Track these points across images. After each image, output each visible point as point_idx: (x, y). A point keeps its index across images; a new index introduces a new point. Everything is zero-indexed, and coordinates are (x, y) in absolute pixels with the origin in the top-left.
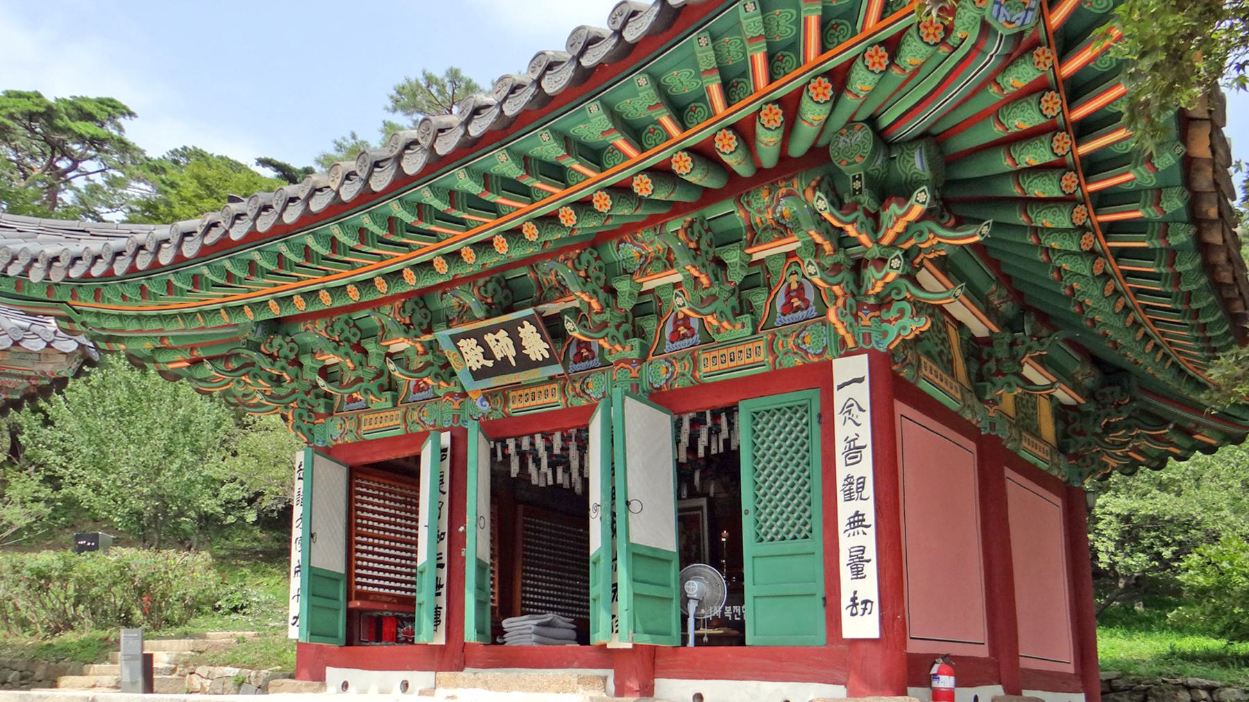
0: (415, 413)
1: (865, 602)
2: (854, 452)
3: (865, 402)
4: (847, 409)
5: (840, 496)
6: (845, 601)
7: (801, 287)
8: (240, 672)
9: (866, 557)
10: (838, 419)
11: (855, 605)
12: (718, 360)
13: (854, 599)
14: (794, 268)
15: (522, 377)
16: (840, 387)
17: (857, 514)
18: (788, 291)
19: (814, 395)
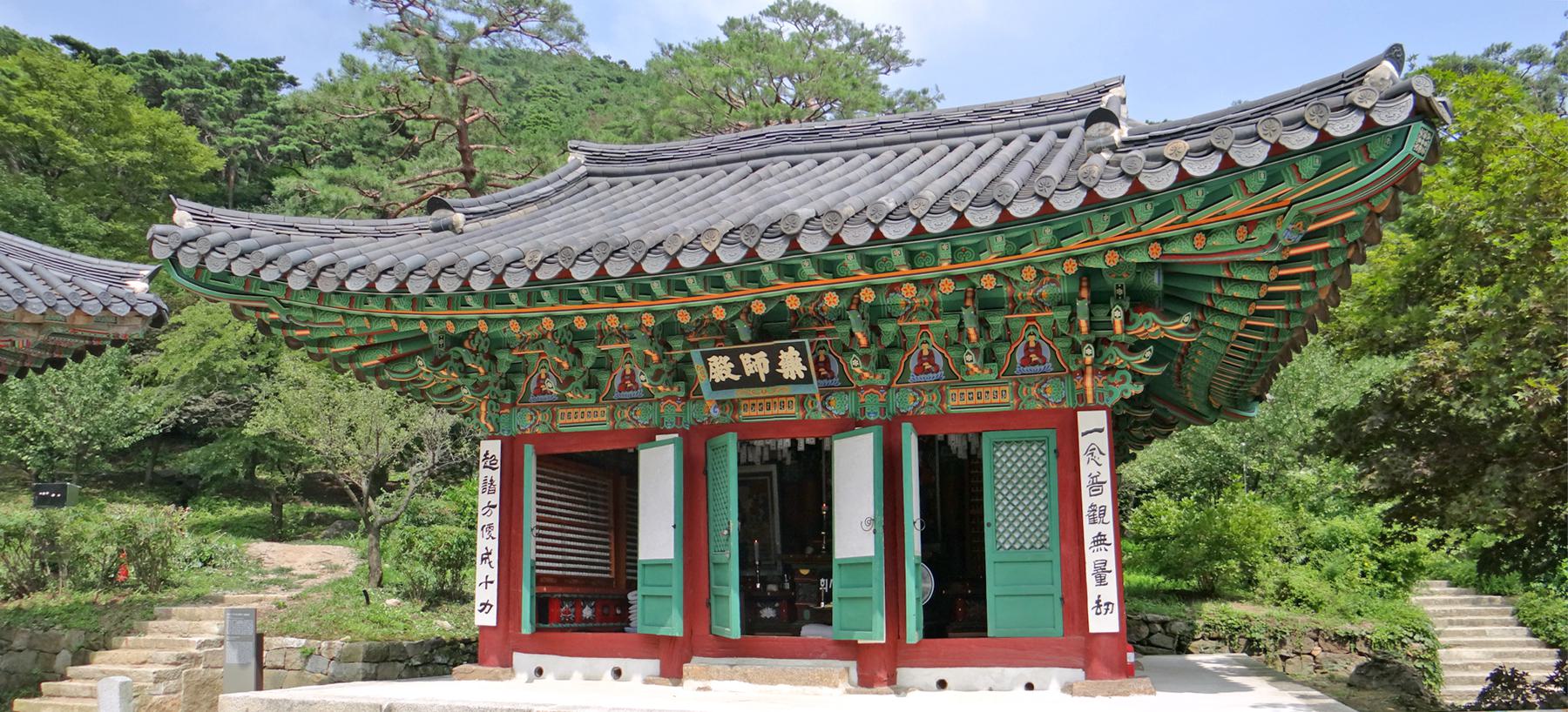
0: (626, 412)
1: (1107, 604)
2: (1096, 485)
3: (1105, 448)
4: (1090, 452)
5: (1086, 520)
6: (1091, 603)
8: (307, 644)
9: (1108, 568)
10: (1083, 459)
11: (1099, 606)
13: (1098, 602)
14: (1031, 330)
15: (770, 391)
16: (1084, 434)
17: (1100, 534)
18: (1027, 347)
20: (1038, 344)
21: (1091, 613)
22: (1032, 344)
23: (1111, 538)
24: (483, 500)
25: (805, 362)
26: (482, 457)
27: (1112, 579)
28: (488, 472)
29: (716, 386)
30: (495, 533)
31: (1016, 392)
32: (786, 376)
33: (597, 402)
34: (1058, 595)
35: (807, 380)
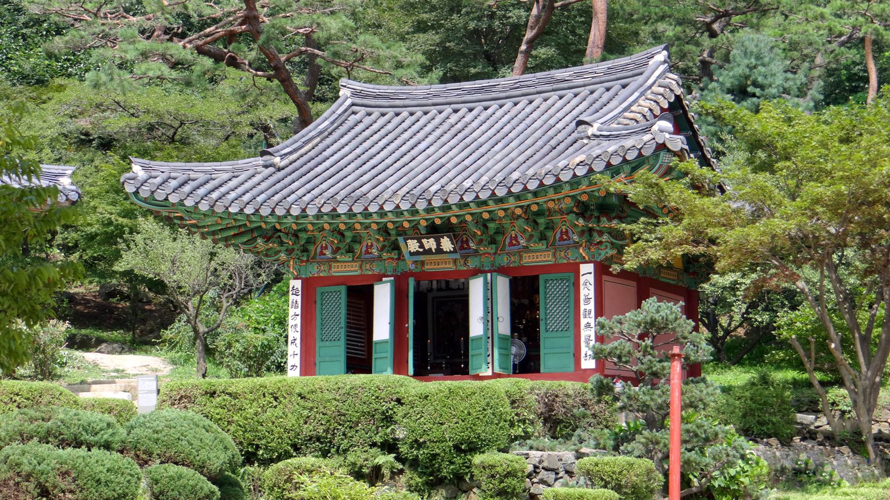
2: (587, 300)
3: (592, 282)
4: (585, 284)
5: (582, 316)
7: (567, 231)
10: (582, 287)
12: (531, 258)
14: (564, 223)
15: (438, 257)
19: (572, 275)
20: (567, 230)
22: (564, 230)
23: (593, 325)
24: (292, 311)
26: (291, 289)
29: (412, 254)
30: (299, 329)
31: (554, 255)
32: (445, 250)
33: (353, 260)
35: (455, 251)
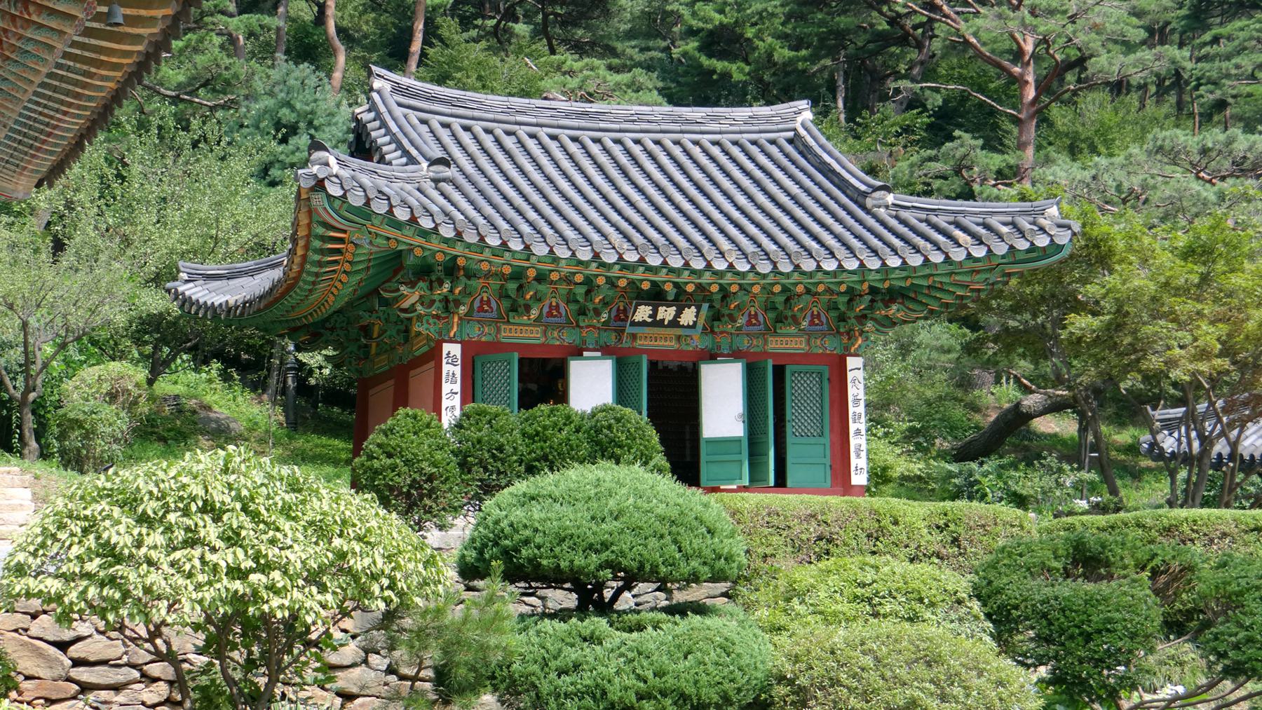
4: (854, 381)
6: (853, 468)
21: (853, 474)
23: (863, 432)
25: (697, 316)
26: (444, 355)
27: (863, 454)
28: (451, 368)
29: (634, 324)
31: (808, 343)
34: (828, 463)
